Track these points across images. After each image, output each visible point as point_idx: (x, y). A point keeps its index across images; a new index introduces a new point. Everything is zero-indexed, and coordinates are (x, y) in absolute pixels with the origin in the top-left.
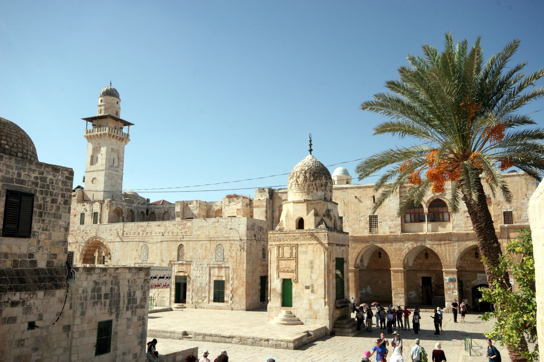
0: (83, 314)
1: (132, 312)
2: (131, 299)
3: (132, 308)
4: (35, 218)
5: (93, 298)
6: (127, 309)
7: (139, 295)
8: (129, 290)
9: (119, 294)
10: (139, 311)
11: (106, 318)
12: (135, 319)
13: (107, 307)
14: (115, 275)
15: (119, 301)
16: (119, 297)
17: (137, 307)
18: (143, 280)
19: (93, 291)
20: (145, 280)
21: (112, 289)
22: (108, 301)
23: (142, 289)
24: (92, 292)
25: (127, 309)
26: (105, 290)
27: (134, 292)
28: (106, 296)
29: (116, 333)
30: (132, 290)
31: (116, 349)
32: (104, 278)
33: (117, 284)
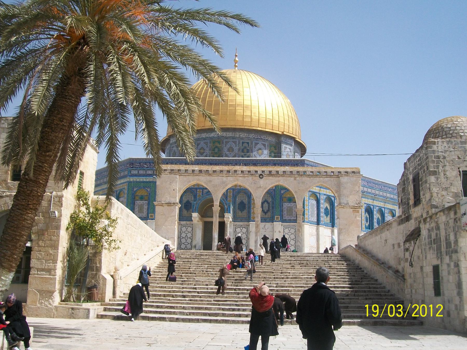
0: (426, 258)
1: (450, 256)
2: (448, 244)
3: (449, 254)
4: (421, 188)
5: (429, 244)
6: (446, 255)
7: (452, 238)
8: (446, 233)
9: (440, 238)
10: (454, 256)
11: (436, 262)
12: (452, 264)
13: (436, 252)
14: (436, 220)
15: (441, 245)
16: (441, 242)
17: (452, 252)
18: (453, 220)
19: (428, 236)
20: (455, 219)
21: (436, 234)
22: (435, 246)
23: (454, 231)
24: (428, 239)
25: (446, 255)
26: (433, 236)
27: (449, 235)
28: (434, 240)
29: (442, 277)
30: (448, 233)
31: (444, 295)
32: (432, 226)
33: (438, 228)
